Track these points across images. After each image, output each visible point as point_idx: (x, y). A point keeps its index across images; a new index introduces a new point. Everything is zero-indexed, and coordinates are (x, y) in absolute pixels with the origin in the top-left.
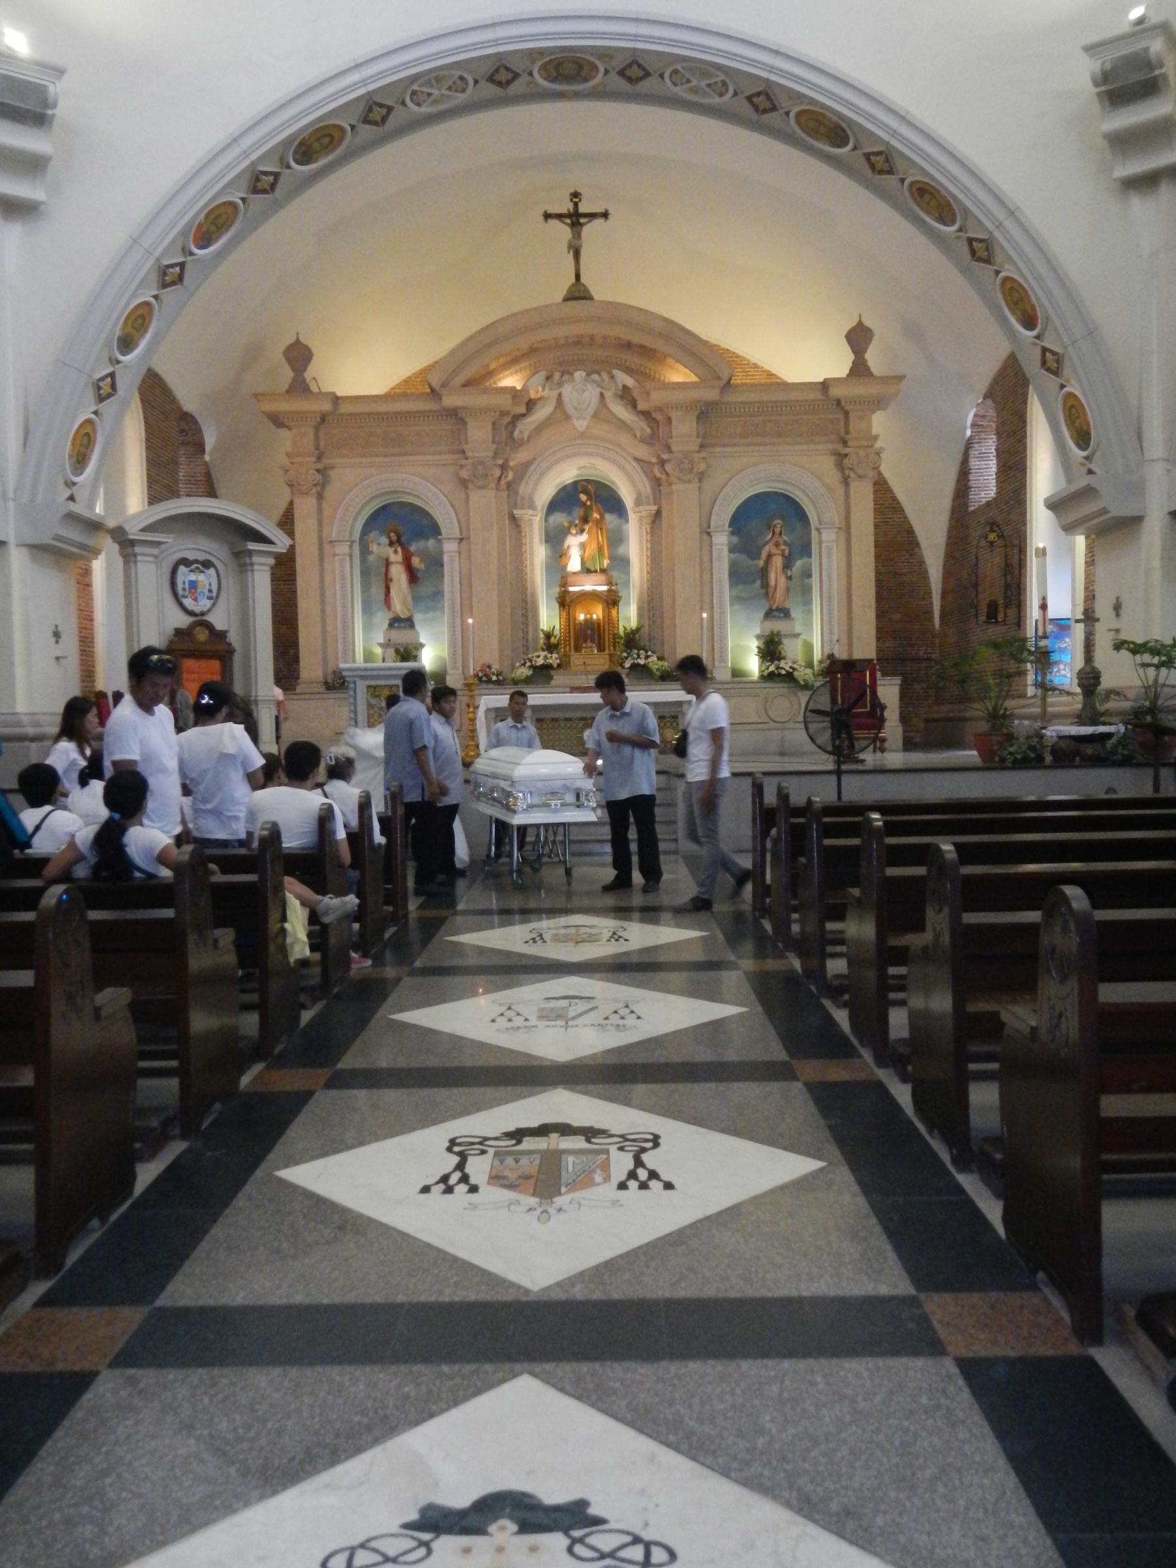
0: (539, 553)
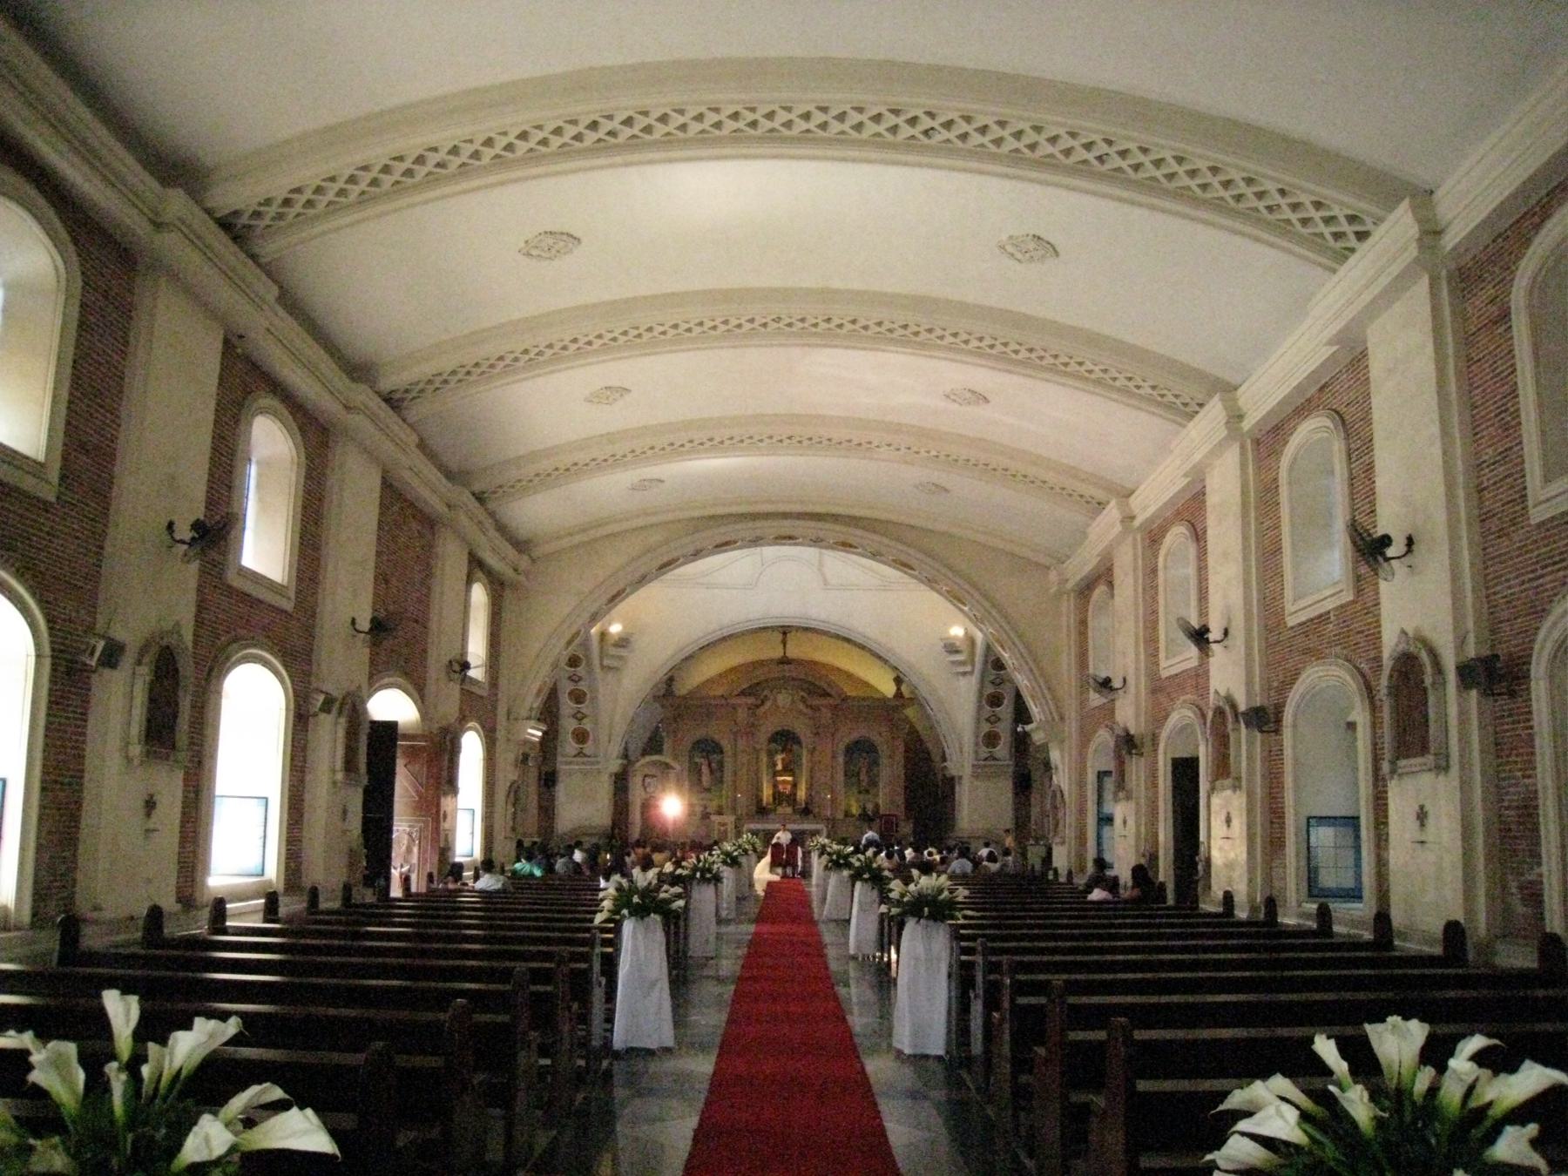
0: (764, 758)
